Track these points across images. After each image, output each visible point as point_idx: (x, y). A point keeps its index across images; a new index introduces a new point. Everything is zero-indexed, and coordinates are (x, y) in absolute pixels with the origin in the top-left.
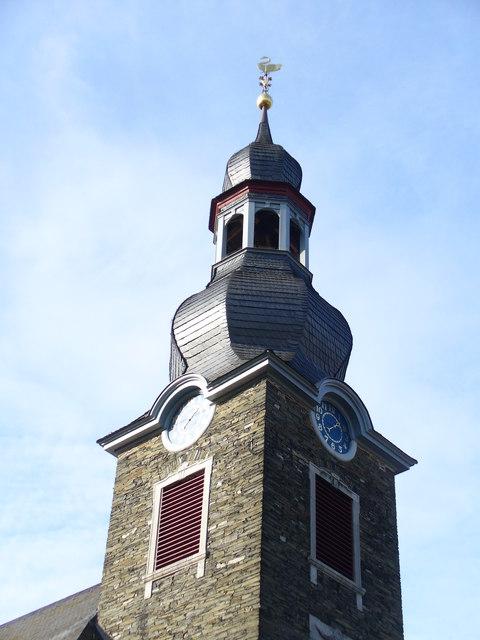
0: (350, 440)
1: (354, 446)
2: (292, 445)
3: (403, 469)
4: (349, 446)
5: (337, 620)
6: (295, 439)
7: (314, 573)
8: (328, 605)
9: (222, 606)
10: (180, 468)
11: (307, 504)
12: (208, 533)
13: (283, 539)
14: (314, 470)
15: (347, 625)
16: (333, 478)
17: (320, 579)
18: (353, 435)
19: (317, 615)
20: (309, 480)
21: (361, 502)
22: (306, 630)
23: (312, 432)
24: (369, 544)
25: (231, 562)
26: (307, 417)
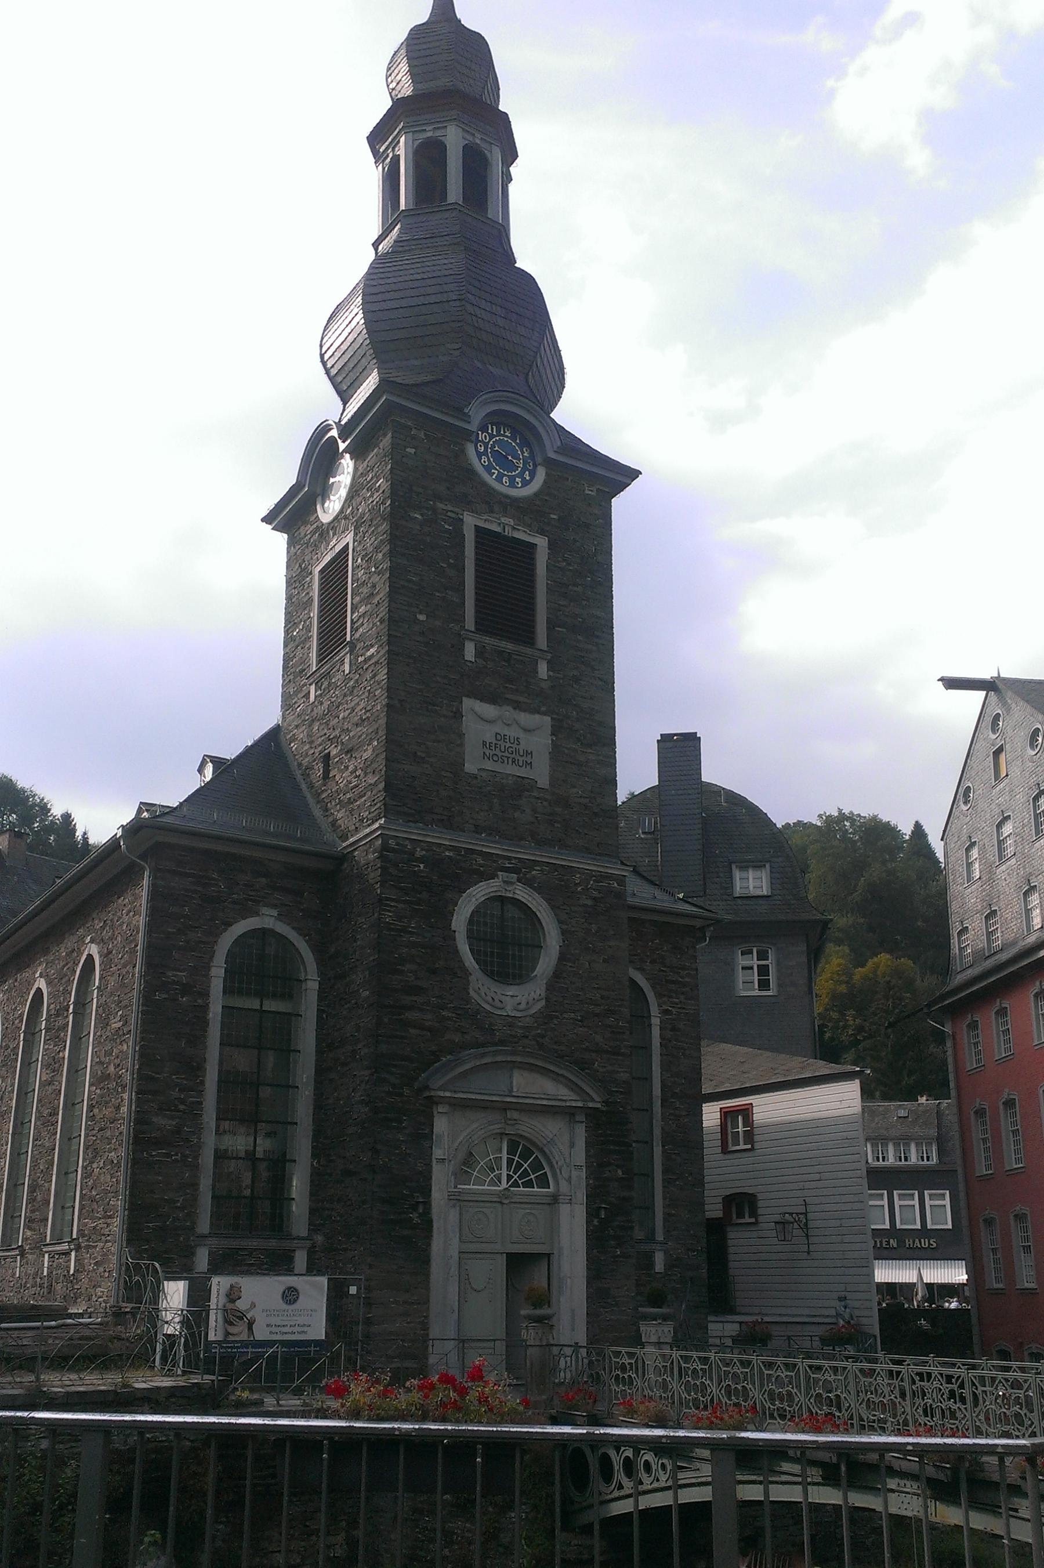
0: (535, 466)
1: (541, 474)
3: (620, 487)
4: (533, 475)
5: (507, 696)
7: (470, 651)
9: (362, 705)
10: (332, 544)
11: (462, 570)
12: (352, 620)
13: (422, 617)
14: (470, 521)
15: (521, 699)
17: (480, 653)
18: (539, 459)
21: (551, 546)
22: (458, 715)
23: (471, 472)
25: (369, 654)
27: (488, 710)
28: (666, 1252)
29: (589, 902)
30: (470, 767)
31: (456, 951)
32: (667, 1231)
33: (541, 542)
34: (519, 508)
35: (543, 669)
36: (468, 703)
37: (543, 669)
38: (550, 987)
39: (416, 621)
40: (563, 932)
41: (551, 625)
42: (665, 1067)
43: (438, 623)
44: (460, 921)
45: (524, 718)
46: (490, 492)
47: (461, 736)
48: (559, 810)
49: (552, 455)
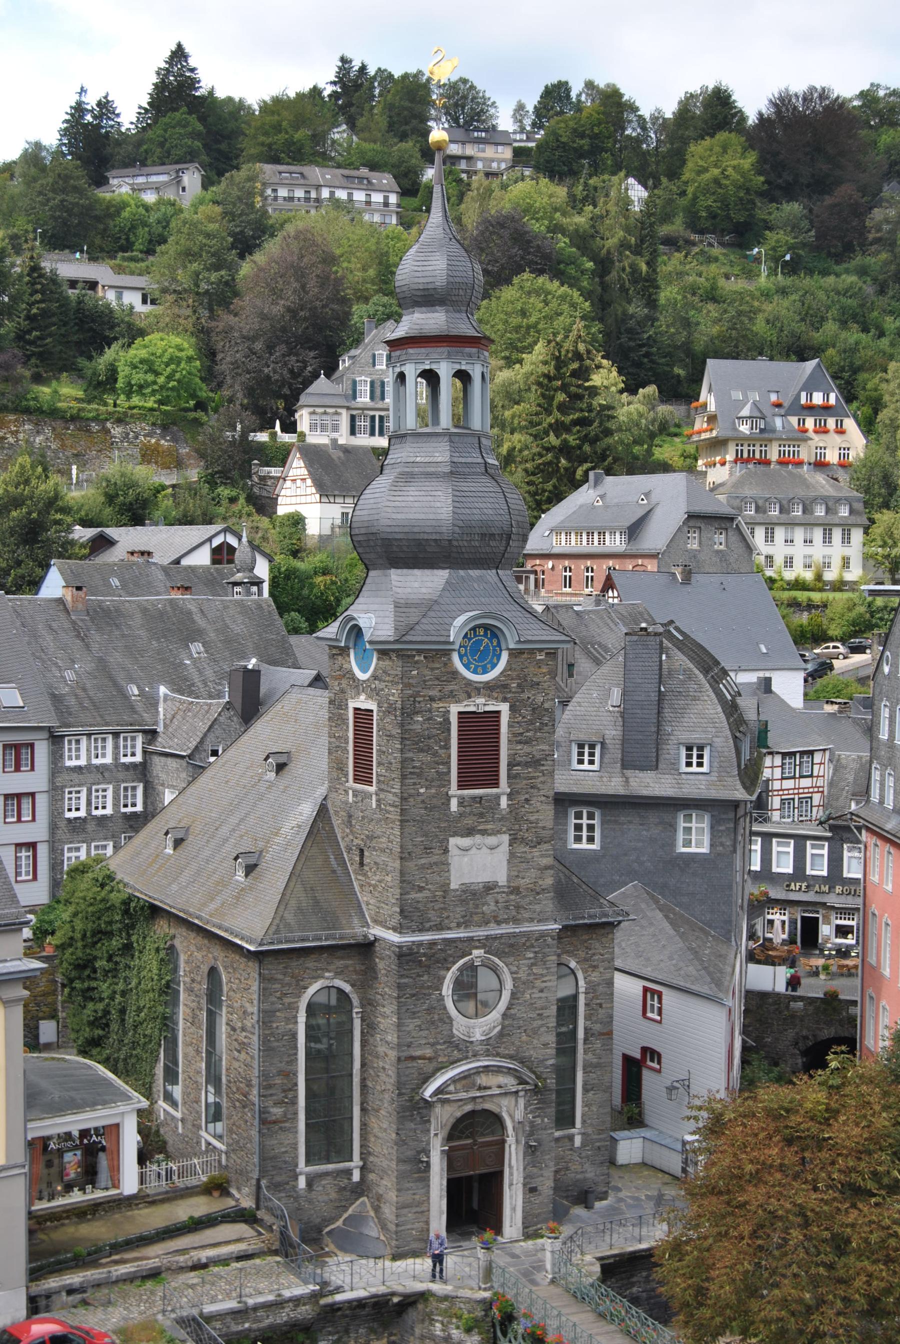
1: (505, 656)
2: (432, 699)
6: (434, 693)
7: (454, 805)
8: (469, 821)
11: (447, 747)
13: (422, 791)
15: (489, 827)
16: (480, 704)
17: (460, 804)
18: (503, 647)
19: (455, 834)
20: (450, 723)
21: (512, 709)
22: (446, 851)
24: (520, 742)
26: (450, 659)
27: (465, 842)
28: (583, 1134)
29: (532, 955)
30: (453, 886)
31: (445, 1008)
32: (584, 1122)
33: (504, 708)
34: (489, 689)
35: (504, 802)
36: (454, 841)
37: (504, 802)
38: (505, 1016)
39: (419, 794)
40: (514, 979)
41: (510, 765)
42: (586, 1018)
43: (433, 791)
44: (447, 989)
45: (491, 840)
46: (469, 683)
47: (448, 864)
48: (512, 897)
49: (512, 646)
